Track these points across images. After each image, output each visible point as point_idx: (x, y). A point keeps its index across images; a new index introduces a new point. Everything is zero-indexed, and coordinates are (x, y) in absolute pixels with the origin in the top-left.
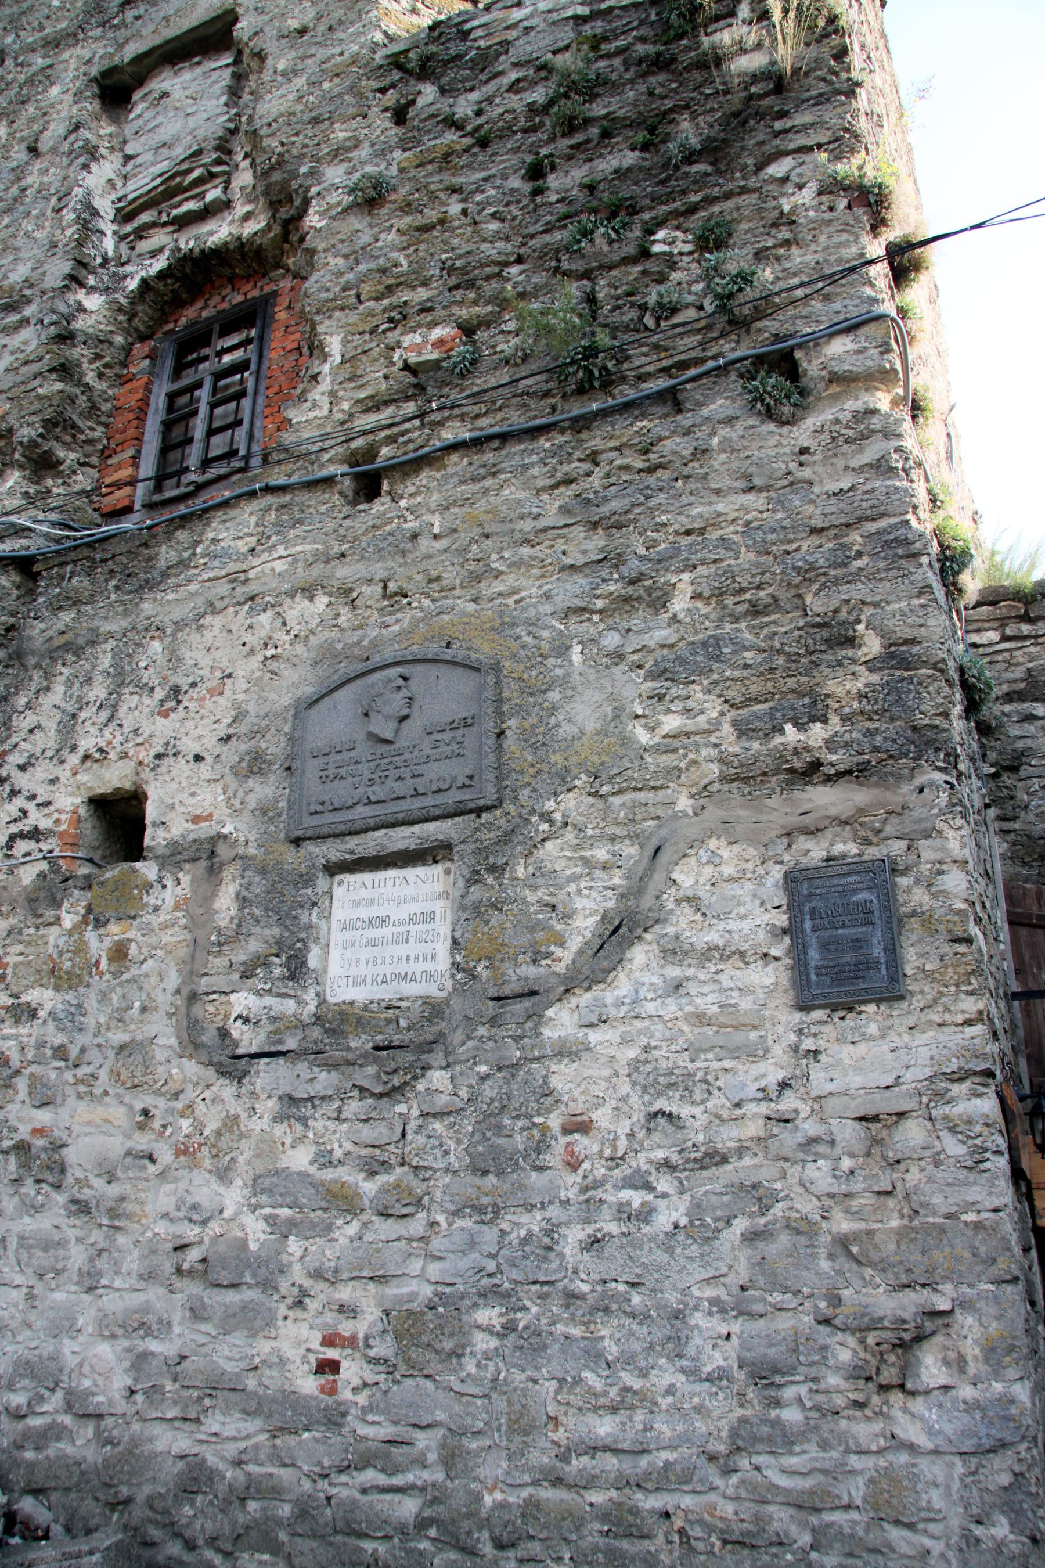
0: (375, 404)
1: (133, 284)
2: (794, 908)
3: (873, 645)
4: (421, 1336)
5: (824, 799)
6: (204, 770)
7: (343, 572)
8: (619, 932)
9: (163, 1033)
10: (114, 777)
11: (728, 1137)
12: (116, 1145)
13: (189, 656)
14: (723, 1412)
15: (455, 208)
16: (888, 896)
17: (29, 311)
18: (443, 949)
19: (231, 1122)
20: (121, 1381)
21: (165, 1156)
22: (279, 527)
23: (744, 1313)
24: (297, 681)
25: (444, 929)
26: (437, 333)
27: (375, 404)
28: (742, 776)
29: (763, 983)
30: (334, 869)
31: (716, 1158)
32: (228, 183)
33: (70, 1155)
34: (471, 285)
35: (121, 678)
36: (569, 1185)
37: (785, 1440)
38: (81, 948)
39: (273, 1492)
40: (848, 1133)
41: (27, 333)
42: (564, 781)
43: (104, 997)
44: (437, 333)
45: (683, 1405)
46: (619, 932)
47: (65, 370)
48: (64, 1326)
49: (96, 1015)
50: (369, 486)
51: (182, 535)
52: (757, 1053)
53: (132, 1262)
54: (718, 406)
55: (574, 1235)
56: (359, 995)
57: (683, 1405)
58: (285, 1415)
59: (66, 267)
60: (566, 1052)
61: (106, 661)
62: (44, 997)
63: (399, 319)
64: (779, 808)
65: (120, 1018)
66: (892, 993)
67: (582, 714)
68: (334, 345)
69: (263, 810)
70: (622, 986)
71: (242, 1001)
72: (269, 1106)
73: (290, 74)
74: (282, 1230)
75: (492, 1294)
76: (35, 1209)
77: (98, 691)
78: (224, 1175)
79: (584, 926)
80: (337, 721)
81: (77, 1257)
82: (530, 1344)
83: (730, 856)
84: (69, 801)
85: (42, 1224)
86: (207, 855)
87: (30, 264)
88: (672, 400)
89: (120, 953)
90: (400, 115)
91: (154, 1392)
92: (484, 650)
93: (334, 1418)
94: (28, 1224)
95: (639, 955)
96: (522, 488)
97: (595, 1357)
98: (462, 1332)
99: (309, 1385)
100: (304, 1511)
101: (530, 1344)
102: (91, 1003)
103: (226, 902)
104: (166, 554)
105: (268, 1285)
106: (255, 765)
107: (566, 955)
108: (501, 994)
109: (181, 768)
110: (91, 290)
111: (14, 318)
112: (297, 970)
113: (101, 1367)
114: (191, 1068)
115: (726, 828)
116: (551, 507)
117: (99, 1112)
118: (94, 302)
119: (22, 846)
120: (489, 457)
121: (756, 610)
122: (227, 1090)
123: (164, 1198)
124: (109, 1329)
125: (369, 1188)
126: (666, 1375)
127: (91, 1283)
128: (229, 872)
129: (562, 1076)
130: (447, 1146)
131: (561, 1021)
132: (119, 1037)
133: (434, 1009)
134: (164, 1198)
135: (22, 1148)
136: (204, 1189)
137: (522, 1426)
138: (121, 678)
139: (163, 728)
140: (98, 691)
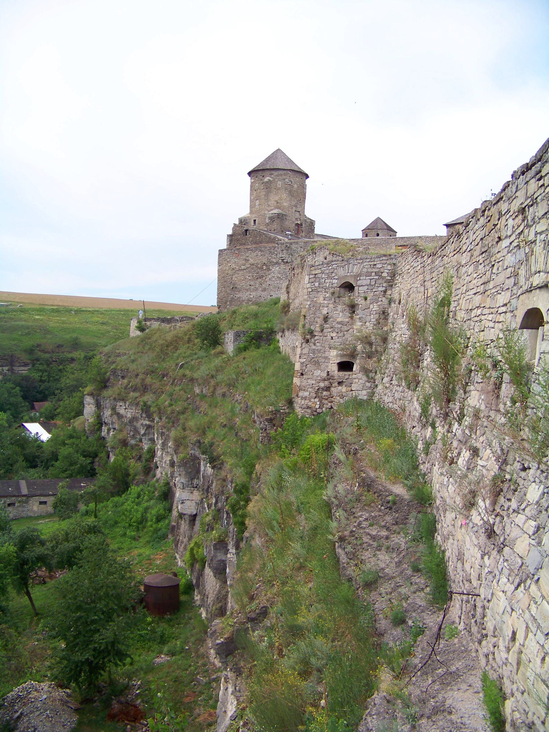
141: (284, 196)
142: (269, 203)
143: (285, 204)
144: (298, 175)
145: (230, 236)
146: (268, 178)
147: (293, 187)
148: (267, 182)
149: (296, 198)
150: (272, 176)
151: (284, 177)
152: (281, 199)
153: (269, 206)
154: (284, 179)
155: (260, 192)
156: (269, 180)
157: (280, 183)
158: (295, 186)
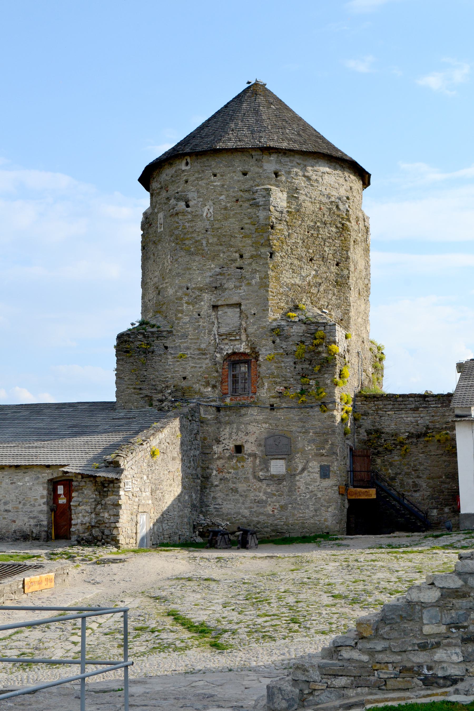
0: (273, 397)
1: (225, 354)
2: (321, 469)
3: (330, 443)
4: (283, 508)
5: (324, 458)
6: (253, 445)
7: (270, 421)
8: (303, 470)
9: (251, 477)
10: (239, 443)
11: (313, 490)
12: (245, 489)
13: (249, 428)
14: (311, 514)
15: (283, 365)
16: (329, 468)
17: (208, 356)
18: (284, 469)
19: (261, 487)
20: (248, 514)
21: (252, 490)
22: (261, 412)
23: (314, 505)
24: (264, 436)
25: (284, 467)
26: (281, 388)
27: (273, 397)
28: (316, 455)
29: (317, 476)
30: (271, 459)
31: (312, 492)
32: (240, 336)
33: (239, 490)
34: (286, 381)
35: (238, 429)
36: (298, 493)
37: (317, 516)
38: (237, 465)
39: (268, 523)
40: (324, 489)
41: (207, 361)
42: (298, 453)
43: (241, 471)
44: (281, 388)
45: (309, 513)
46: (303, 470)
47: (217, 371)
48: (240, 508)
49: (240, 474)
50: (272, 408)
51: (245, 409)
52: (316, 482)
53: (249, 501)
54: (316, 409)
55: (298, 498)
56: (275, 473)
57: (309, 513)
58: (268, 516)
59: (214, 350)
60: (298, 481)
61: (235, 426)
62: (232, 471)
63: (276, 383)
64: (320, 458)
65: (244, 474)
66: (329, 478)
67: (300, 445)
68: (266, 384)
69: (262, 451)
70: (304, 475)
71: (261, 473)
72: (265, 485)
73: (254, 324)
74: (268, 498)
75: (291, 504)
76: (235, 496)
77: (234, 431)
78: (260, 492)
79: (300, 468)
80: (271, 441)
81: (241, 501)
82: (294, 508)
83: (315, 463)
84: (232, 446)
85: (236, 497)
86: (254, 455)
87: (205, 345)
88: (312, 407)
89: (243, 466)
90: (274, 342)
91: (253, 515)
92: (289, 436)
93: (274, 516)
94: (233, 497)
95: (305, 472)
96: (294, 415)
97: (300, 509)
98: (287, 507)
99: (271, 513)
100: (271, 524)
101: (294, 508)
102: (239, 472)
103: (258, 461)
104: (243, 411)
105: (266, 503)
106: (260, 445)
107: (298, 471)
108: (291, 474)
109: (249, 444)
110: (217, 352)
111: (204, 357)
112: (268, 470)
113: (246, 512)
114: (255, 480)
115: (314, 460)
116: (297, 418)
117: (242, 485)
118: (218, 355)
119: (225, 451)
120: (289, 410)
121: (319, 436)
122: (260, 483)
123: (252, 494)
124: (246, 508)
125: (277, 494)
126: (307, 511)
127: (243, 503)
128: (258, 458)
129: (297, 483)
130: (286, 489)
131: (297, 478)
132: (244, 476)
133: (284, 476)
134: (252, 494)
135: (231, 489)
136: (258, 494)
137: (294, 515)
138: (238, 429)
139: (246, 438)
140: (234, 431)
147: (196, 216)
158: (207, 210)
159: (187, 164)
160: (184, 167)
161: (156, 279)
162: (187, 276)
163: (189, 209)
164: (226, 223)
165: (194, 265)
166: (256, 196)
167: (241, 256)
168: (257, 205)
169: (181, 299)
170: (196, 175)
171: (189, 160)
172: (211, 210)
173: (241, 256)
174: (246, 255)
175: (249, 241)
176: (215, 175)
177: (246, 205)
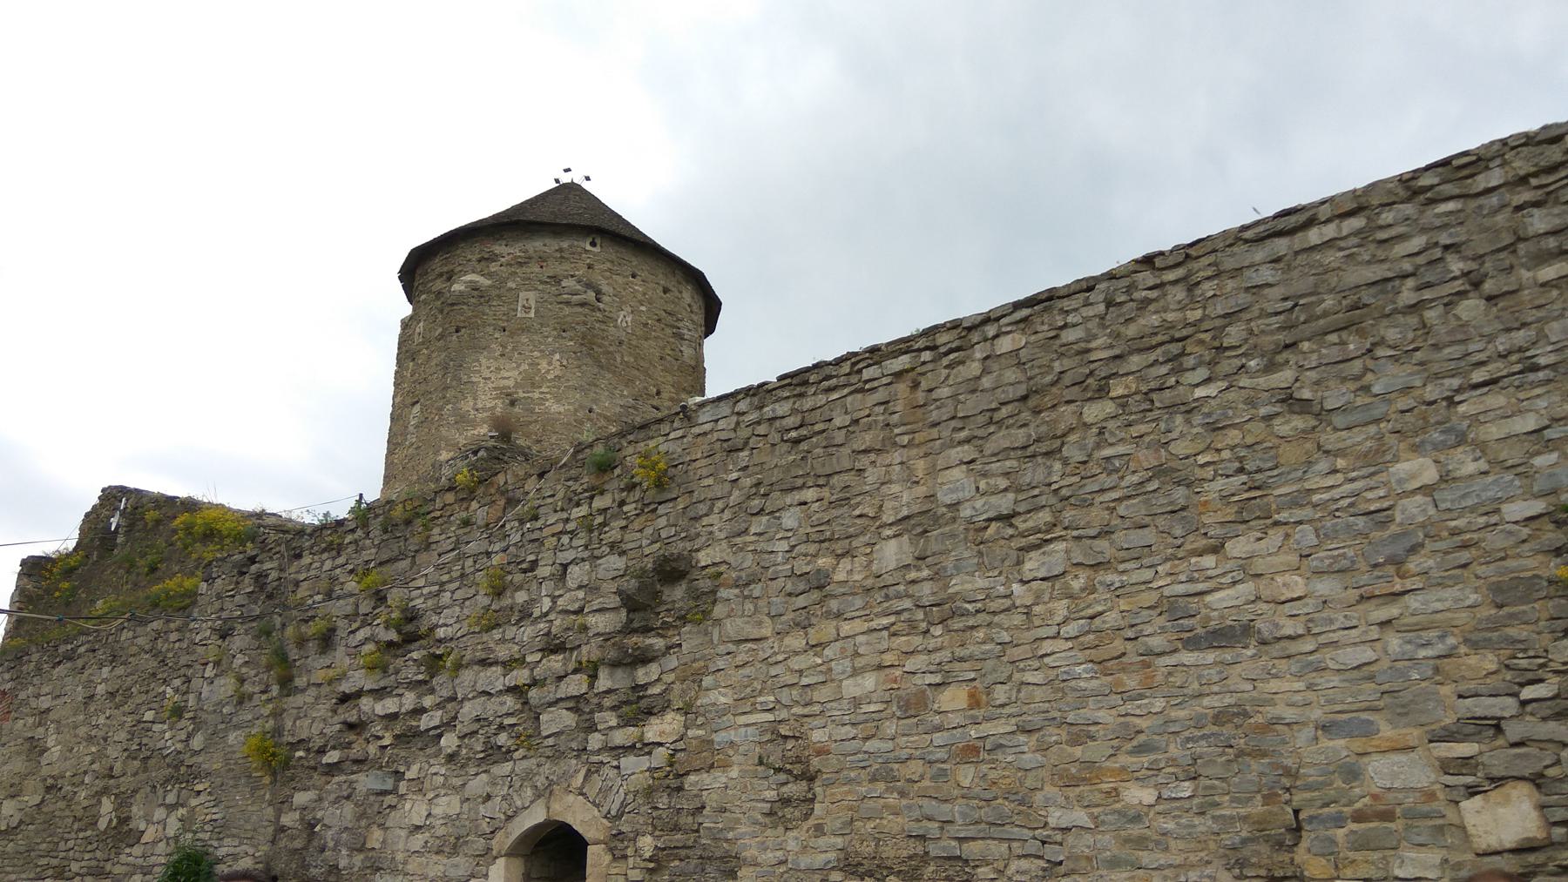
141: (551, 367)
142: (467, 405)
143: (555, 408)
144: (635, 262)
145: (33, 568)
146: (469, 277)
147: (608, 319)
148: (460, 300)
149: (629, 382)
150: (494, 267)
151: (554, 268)
152: (531, 382)
153: (463, 420)
154: (556, 280)
155: (429, 358)
156: (475, 288)
157: (529, 297)
158: (625, 318)
159: (593, 244)
160: (588, 247)
161: (511, 383)
162: (592, 395)
163: (601, 306)
164: (646, 344)
165: (603, 383)
166: (680, 324)
167: (658, 393)
168: (681, 337)
169: (581, 423)
170: (608, 265)
171: (598, 241)
172: (629, 319)
173: (658, 393)
174: (665, 395)
175: (670, 378)
176: (634, 276)
177: (669, 331)
